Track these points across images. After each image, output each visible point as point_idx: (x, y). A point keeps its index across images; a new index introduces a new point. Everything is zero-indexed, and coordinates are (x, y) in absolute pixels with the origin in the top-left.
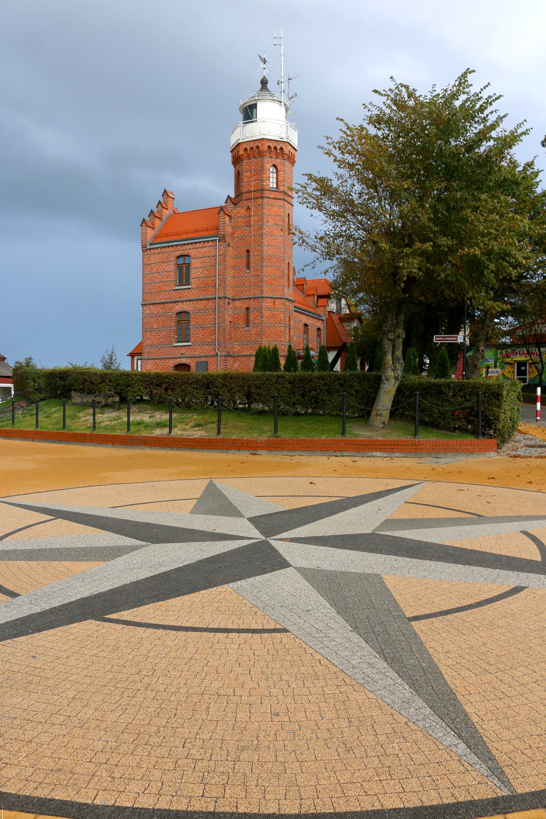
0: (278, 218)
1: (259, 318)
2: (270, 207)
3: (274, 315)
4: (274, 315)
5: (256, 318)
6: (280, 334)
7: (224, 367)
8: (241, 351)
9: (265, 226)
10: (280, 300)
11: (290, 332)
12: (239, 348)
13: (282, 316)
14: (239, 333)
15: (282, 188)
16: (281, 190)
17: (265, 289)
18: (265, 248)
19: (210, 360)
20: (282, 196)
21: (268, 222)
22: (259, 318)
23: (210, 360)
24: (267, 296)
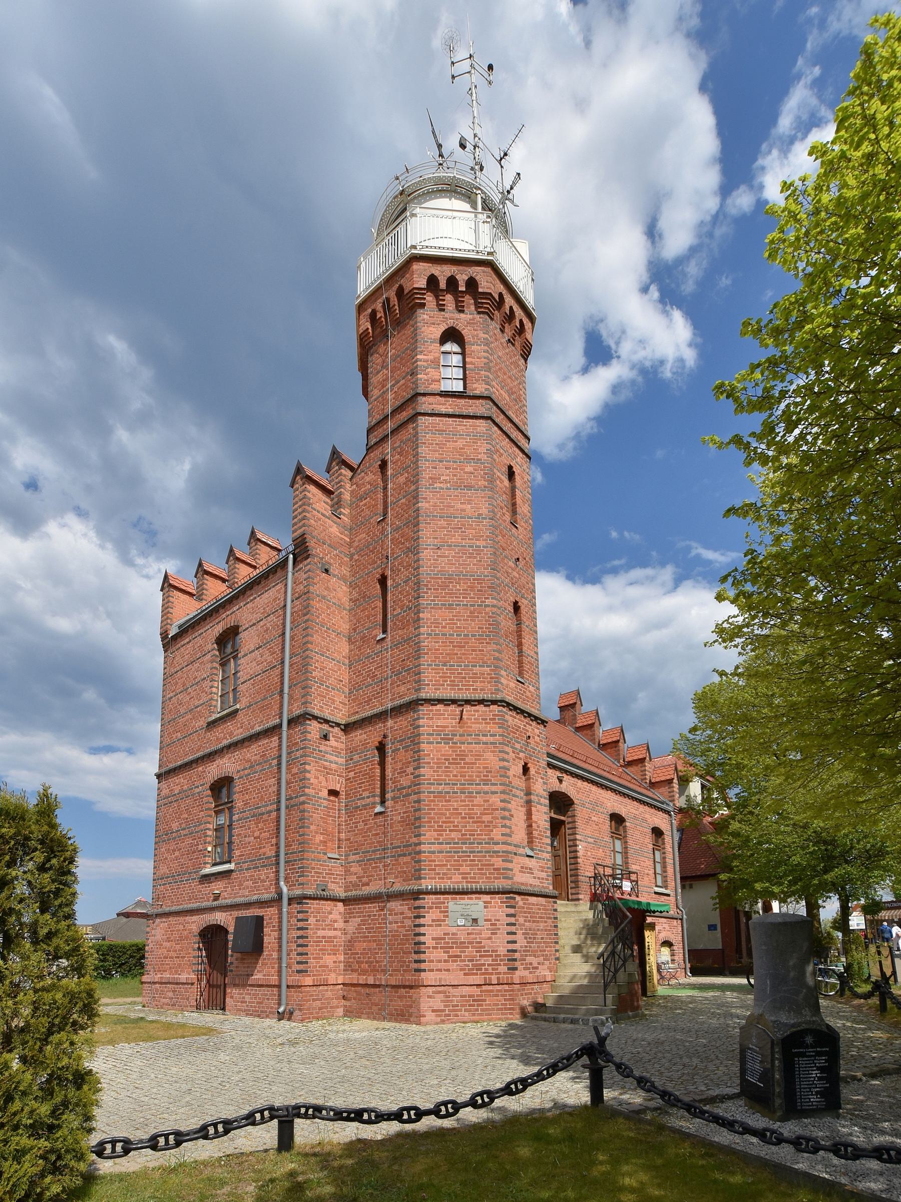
0: (469, 469)
1: (410, 770)
2: (439, 438)
3: (462, 756)
4: (462, 756)
5: (402, 772)
6: (486, 818)
7: (300, 933)
8: (365, 880)
9: (424, 492)
10: (481, 708)
11: (529, 814)
12: (361, 873)
13: (492, 759)
14: (361, 825)
15: (479, 388)
16: (477, 392)
17: (429, 675)
18: (426, 554)
19: (269, 913)
20: (480, 408)
21: (434, 479)
22: (410, 770)
23: (269, 913)
24: (438, 695)
